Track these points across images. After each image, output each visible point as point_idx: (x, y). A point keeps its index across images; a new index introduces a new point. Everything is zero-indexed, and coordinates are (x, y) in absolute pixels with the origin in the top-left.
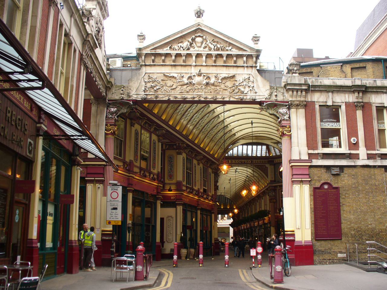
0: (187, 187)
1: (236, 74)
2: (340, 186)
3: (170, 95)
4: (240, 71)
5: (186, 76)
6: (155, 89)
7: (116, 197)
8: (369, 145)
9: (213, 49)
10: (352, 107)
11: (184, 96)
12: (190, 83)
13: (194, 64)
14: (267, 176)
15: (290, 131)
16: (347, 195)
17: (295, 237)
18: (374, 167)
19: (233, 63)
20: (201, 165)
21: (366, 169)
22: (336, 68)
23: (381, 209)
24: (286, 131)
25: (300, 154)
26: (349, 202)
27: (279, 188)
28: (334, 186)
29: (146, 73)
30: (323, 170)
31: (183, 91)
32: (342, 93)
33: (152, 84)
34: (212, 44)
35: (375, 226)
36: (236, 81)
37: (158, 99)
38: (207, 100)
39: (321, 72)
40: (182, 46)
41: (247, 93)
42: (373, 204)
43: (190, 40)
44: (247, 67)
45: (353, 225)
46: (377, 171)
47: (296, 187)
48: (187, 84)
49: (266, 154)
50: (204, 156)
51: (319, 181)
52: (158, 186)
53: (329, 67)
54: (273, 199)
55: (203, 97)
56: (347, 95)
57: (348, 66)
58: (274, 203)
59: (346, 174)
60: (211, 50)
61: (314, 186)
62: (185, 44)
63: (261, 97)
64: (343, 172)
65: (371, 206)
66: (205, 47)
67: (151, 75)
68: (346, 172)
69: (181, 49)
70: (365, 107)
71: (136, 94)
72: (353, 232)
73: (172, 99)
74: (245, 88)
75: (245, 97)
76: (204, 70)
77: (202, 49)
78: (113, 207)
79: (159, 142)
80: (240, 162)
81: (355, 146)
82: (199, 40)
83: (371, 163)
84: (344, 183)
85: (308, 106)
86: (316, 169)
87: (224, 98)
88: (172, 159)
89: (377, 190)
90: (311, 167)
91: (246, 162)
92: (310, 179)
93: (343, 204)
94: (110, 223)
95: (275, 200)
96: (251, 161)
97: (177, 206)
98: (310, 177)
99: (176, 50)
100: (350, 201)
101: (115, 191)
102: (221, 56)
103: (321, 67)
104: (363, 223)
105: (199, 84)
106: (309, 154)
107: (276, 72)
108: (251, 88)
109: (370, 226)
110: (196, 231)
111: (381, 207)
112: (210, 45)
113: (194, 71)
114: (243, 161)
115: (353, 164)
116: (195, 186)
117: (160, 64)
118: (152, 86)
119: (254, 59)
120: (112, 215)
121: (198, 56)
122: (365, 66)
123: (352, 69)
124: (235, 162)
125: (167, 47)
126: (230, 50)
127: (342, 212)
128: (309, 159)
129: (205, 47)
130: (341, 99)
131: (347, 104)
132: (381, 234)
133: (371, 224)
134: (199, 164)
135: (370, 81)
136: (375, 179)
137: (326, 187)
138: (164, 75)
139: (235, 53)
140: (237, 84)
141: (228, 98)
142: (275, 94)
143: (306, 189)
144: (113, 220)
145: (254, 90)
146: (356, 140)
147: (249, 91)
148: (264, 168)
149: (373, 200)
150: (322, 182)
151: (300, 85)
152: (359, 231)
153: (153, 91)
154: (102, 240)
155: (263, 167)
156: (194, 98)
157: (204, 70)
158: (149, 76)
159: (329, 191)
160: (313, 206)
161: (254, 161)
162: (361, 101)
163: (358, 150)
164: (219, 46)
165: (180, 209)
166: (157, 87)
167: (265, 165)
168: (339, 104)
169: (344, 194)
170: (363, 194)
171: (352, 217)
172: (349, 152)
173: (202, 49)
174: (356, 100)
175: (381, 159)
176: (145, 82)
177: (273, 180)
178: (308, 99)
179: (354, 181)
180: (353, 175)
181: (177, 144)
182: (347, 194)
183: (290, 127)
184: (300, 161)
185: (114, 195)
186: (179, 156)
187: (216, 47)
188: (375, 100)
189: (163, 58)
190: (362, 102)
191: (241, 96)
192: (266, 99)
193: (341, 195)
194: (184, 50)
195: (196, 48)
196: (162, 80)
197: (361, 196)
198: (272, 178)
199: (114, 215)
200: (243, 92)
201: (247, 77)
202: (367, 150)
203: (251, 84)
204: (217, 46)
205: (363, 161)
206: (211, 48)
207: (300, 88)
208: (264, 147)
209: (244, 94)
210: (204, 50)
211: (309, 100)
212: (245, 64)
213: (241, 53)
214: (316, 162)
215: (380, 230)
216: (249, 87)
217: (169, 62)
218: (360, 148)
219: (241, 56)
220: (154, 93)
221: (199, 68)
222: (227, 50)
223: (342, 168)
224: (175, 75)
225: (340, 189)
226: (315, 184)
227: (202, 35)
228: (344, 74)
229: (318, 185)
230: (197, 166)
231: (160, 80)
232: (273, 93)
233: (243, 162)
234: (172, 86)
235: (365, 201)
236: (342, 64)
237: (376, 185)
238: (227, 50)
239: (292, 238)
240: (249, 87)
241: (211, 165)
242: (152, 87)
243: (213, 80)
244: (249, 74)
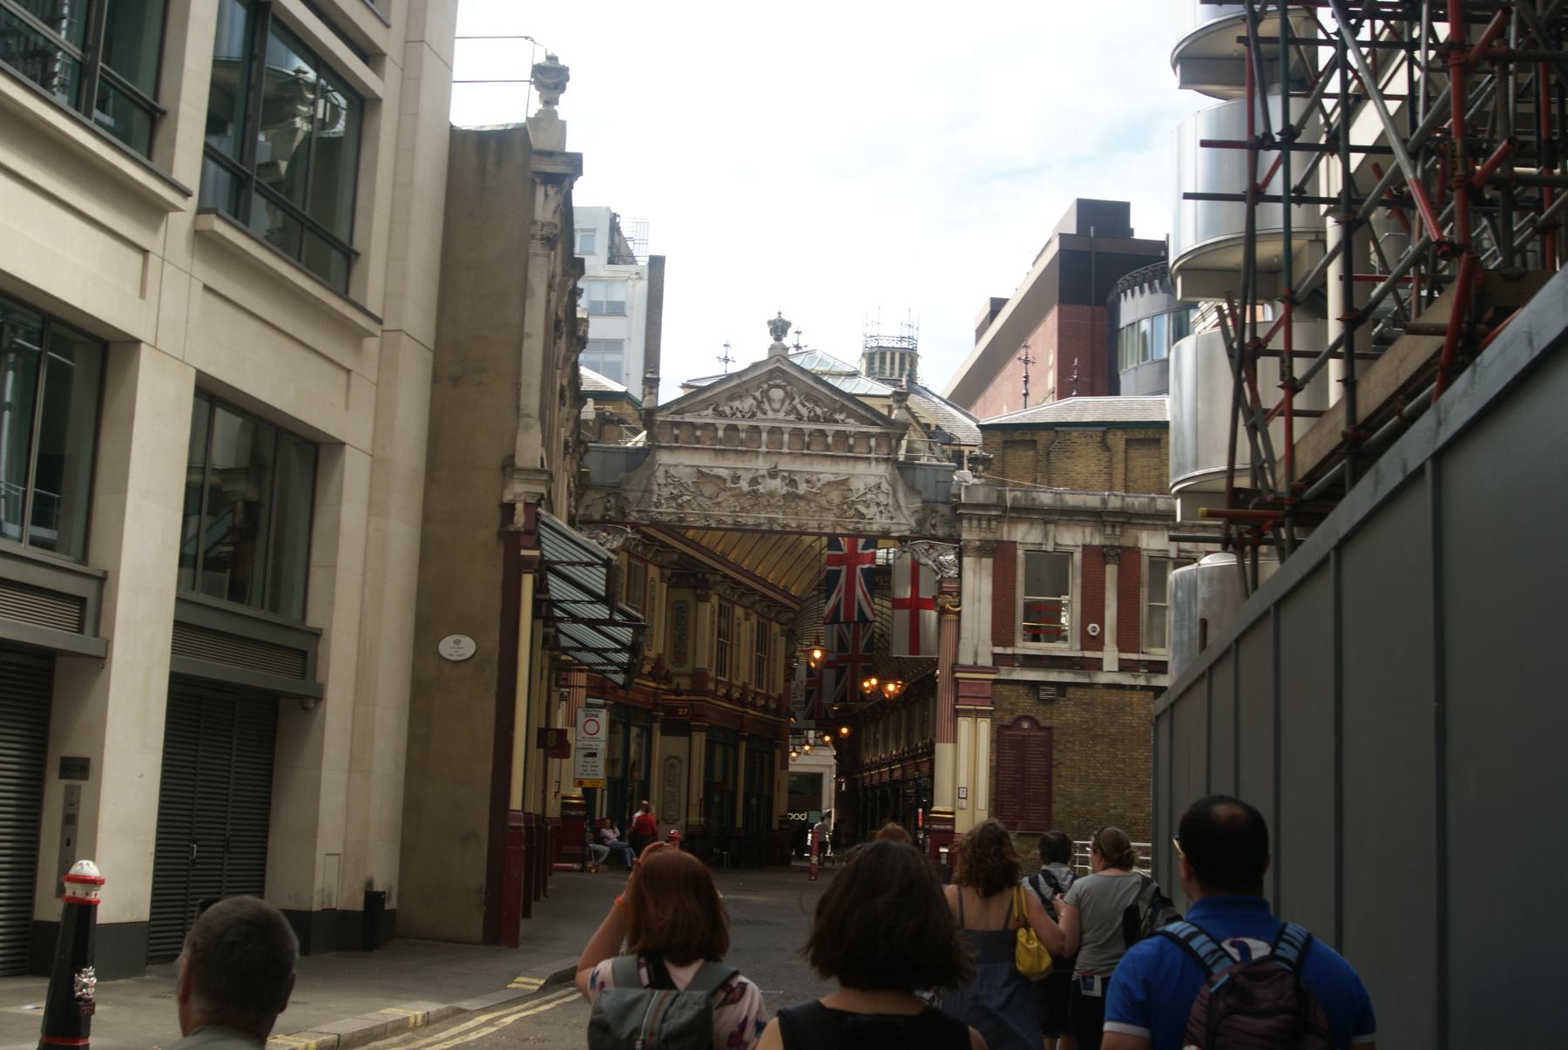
0: (717, 682)
1: (853, 475)
2: (1055, 725)
3: (710, 516)
4: (861, 468)
5: (748, 476)
6: (680, 501)
7: (596, 729)
8: (1127, 640)
9: (806, 419)
10: (1095, 557)
11: (740, 519)
12: (754, 491)
13: (764, 449)
15: (959, 605)
16: (1069, 745)
17: (954, 826)
18: (1133, 688)
19: (846, 449)
20: (754, 618)
21: (1114, 691)
22: (1091, 437)
23: (1139, 776)
24: (949, 602)
25: (976, 654)
26: (1071, 760)
28: (1043, 724)
29: (660, 465)
30: (1022, 690)
31: (738, 509)
32: (1078, 525)
33: (674, 491)
34: (804, 406)
35: (1122, 811)
36: (851, 490)
37: (684, 524)
38: (788, 529)
39: (1056, 444)
40: (741, 409)
41: (872, 519)
42: (1122, 766)
43: (758, 394)
44: (877, 460)
45: (1076, 806)
46: (1136, 697)
47: (964, 724)
48: (749, 492)
50: (764, 596)
51: (1012, 712)
52: (657, 689)
53: (1075, 434)
55: (779, 524)
56: (1088, 531)
57: (1119, 433)
59: (1070, 700)
60: (800, 420)
61: (1001, 723)
62: (748, 403)
63: (903, 528)
64: (1064, 695)
65: (1118, 768)
66: (787, 413)
67: (672, 471)
68: (1070, 696)
69: (739, 414)
70: (1127, 557)
71: (639, 511)
72: (1075, 822)
73: (714, 526)
74: (868, 507)
75: (868, 528)
76: (785, 465)
77: (781, 415)
78: (586, 751)
79: (662, 581)
81: (1096, 642)
82: (777, 394)
83: (1126, 679)
84: (1064, 718)
85: (1000, 554)
86: (1007, 687)
87: (822, 528)
88: (684, 612)
89: (1134, 737)
90: (996, 682)
91: (881, 584)
92: (992, 708)
93: (1061, 764)
94: (580, 783)
97: (693, 733)
98: (993, 704)
99: (726, 416)
100: (1074, 758)
101: (592, 719)
102: (823, 433)
103: (1057, 432)
104: (1098, 804)
105: (771, 494)
106: (995, 655)
107: (941, 468)
108: (882, 508)
109: (1112, 811)
110: (734, 794)
111: (1141, 773)
112: (800, 407)
113: (762, 465)
115: (1087, 681)
116: (737, 677)
117: (691, 446)
118: (672, 494)
119: (894, 442)
120: (585, 768)
121: (773, 431)
122: (1157, 436)
123: (1129, 442)
125: (707, 408)
126: (843, 421)
127: (1055, 779)
128: (994, 664)
129: (787, 413)
130: (1072, 538)
131: (1086, 548)
132: (1134, 827)
133: (1115, 808)
134: (747, 617)
135: (1142, 500)
136: (1132, 714)
137: (1026, 725)
138: (700, 472)
139: (852, 429)
140: (854, 499)
141: (831, 527)
142: (933, 521)
143: (984, 726)
144: (587, 777)
145: (889, 512)
146: (1098, 629)
147: (878, 514)
149: (1124, 756)
150: (1019, 713)
151: (985, 506)
152: (1089, 820)
153: (674, 505)
154: (564, 817)
156: (760, 524)
157: (785, 465)
158: (666, 472)
159: (1032, 733)
160: (994, 764)
162: (1117, 544)
163: (1101, 650)
164: (819, 411)
165: (699, 739)
166: (685, 498)
168: (1070, 550)
169: (1063, 742)
170: (1103, 743)
171: (1077, 790)
172: (1080, 654)
173: (781, 415)
174: (1108, 543)
175: (1150, 672)
176: (659, 485)
178: (1002, 536)
179: (1087, 716)
180: (1086, 704)
181: (700, 575)
182: (1070, 742)
183: (959, 594)
184: (975, 668)
185: (591, 727)
186: (701, 604)
187: (812, 414)
188: (1148, 544)
189: (698, 433)
190: (1120, 547)
191: (860, 526)
192: (912, 532)
193: (1055, 744)
194: (743, 416)
195: (770, 414)
196: (694, 482)
197: (1098, 748)
199: (589, 768)
200: (862, 516)
201: (872, 481)
202: (1120, 651)
203: (882, 499)
204: (815, 412)
205: (1110, 672)
206: (802, 416)
207: (987, 513)
209: (866, 521)
210: (787, 418)
211: (1005, 538)
212: (873, 452)
213: (865, 429)
214: (1004, 674)
215: (1133, 821)
216: (878, 504)
217: (709, 443)
218: (1105, 648)
219: (868, 435)
220: (676, 511)
221: (775, 459)
222: (836, 421)
223: (1062, 687)
224: (724, 473)
225: (1055, 731)
226: (1001, 718)
227: (783, 384)
228: (1107, 454)
229: (1008, 720)
230: (742, 624)
231: (690, 483)
232: (929, 520)
234: (716, 497)
235: (1108, 759)
236: (1104, 429)
237: (1132, 727)
238: (836, 421)
239: (949, 827)
240: (878, 504)
241: (779, 613)
242: (673, 497)
243: (803, 488)
244: (881, 476)
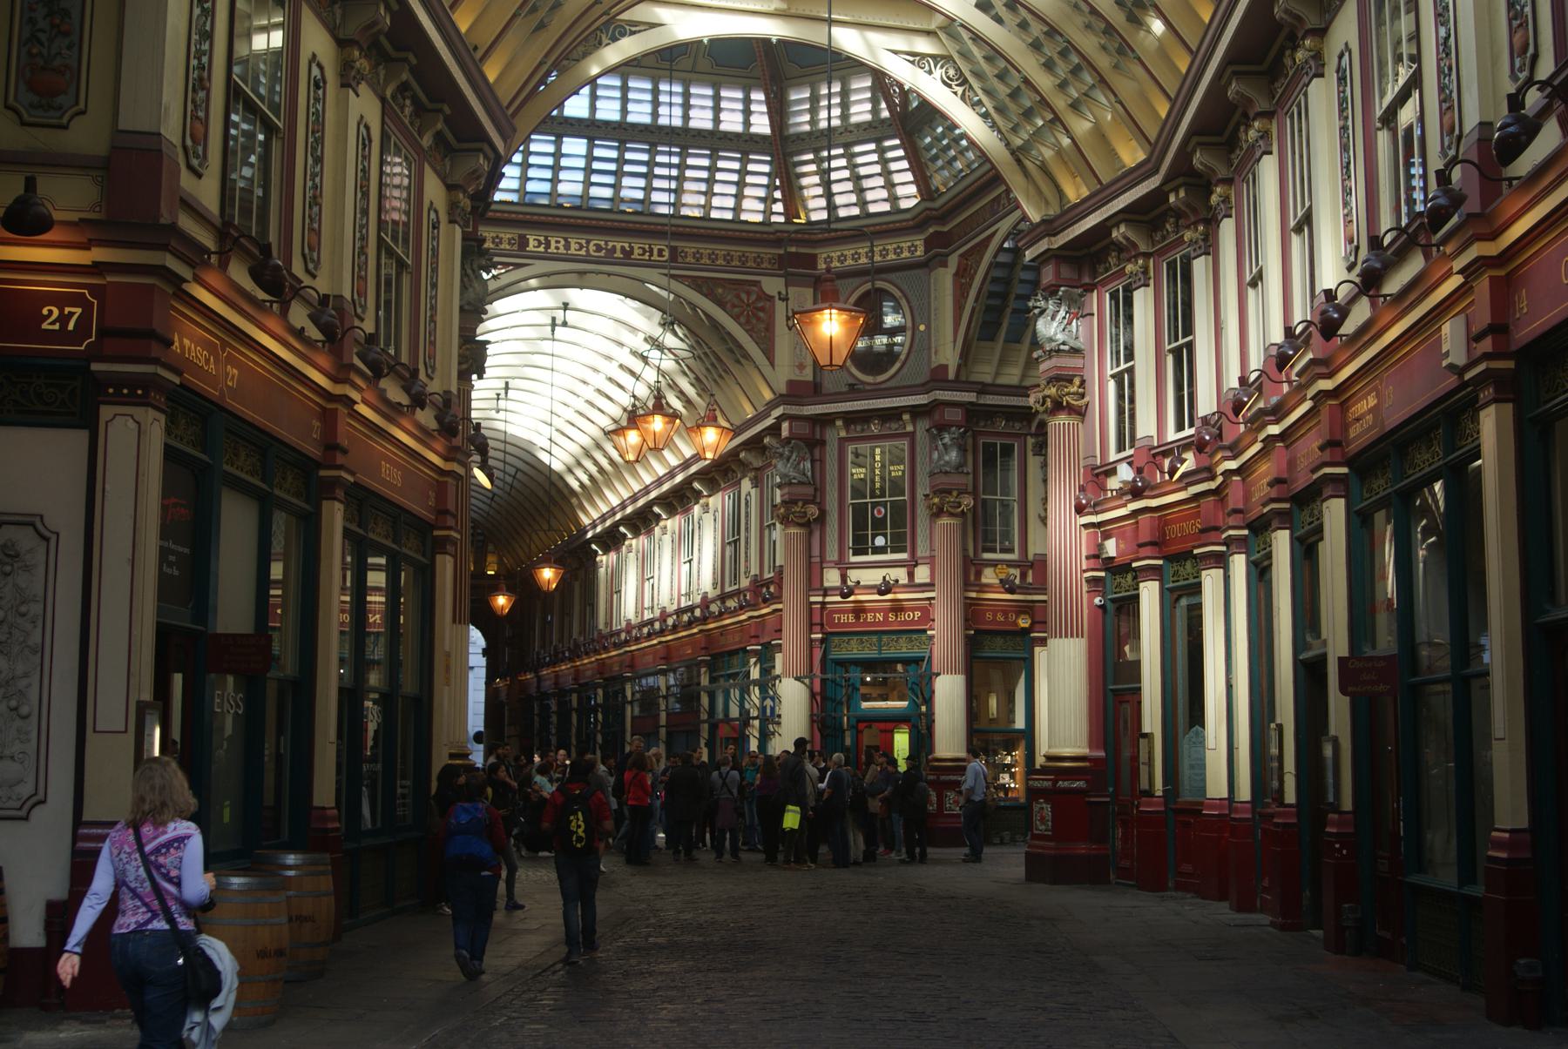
14: (769, 354)
27: (843, 434)
49: (768, 212)
54: (806, 502)
58: (807, 525)
80: (599, 248)
91: (635, 256)
95: (813, 511)
96: (673, 250)
114: (619, 244)
124: (567, 246)
148: (753, 297)
155: (744, 296)
161: (689, 247)
167: (759, 282)
177: (807, 383)
198: (801, 367)
208: (760, 167)
233: (618, 254)
